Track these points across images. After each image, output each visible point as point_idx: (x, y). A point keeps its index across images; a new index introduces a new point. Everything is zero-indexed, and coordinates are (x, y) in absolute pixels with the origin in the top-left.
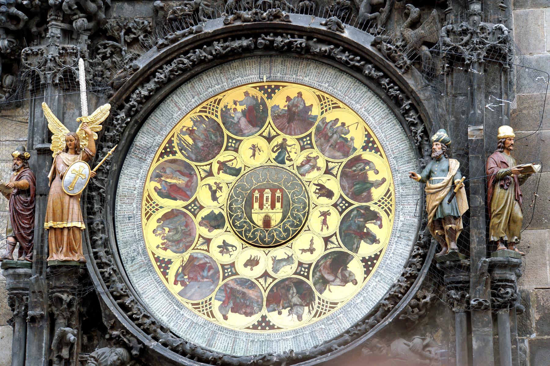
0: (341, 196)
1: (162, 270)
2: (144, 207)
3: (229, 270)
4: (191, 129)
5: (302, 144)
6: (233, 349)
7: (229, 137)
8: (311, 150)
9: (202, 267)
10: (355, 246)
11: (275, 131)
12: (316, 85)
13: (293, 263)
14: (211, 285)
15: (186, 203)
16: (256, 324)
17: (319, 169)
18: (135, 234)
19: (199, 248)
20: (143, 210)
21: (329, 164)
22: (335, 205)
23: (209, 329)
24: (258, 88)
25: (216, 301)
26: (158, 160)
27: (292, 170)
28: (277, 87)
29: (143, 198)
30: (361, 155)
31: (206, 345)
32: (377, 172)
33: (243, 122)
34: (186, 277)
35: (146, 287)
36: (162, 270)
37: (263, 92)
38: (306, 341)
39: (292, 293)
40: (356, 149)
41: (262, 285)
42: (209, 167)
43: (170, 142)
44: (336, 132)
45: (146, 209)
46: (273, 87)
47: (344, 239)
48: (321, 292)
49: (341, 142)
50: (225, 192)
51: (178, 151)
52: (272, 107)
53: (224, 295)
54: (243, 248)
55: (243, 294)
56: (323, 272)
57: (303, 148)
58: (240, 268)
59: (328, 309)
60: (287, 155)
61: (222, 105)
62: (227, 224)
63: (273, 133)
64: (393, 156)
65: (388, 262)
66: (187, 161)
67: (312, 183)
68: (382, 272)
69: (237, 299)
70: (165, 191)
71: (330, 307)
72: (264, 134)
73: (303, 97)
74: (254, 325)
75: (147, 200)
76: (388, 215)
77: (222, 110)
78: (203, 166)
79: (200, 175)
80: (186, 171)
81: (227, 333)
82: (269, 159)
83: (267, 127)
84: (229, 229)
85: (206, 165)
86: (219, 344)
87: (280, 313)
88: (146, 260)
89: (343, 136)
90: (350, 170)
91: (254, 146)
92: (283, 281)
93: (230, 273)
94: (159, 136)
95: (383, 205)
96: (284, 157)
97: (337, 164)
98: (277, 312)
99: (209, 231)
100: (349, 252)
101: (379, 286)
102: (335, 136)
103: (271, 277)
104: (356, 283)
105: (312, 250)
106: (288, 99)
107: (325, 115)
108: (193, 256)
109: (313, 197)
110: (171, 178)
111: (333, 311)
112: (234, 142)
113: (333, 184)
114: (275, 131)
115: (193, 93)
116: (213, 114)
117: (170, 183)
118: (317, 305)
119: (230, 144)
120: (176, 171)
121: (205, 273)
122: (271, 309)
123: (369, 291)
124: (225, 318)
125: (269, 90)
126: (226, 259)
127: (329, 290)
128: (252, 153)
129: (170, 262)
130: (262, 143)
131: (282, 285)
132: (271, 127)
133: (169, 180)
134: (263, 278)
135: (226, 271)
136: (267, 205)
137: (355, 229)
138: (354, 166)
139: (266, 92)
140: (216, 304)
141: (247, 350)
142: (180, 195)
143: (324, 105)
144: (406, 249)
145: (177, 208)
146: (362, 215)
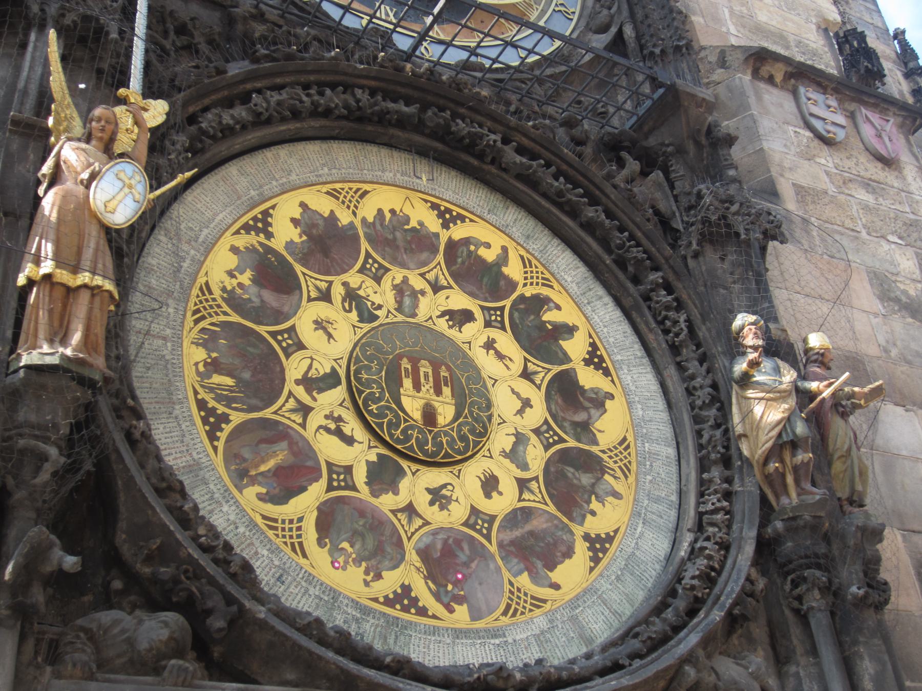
2: (279, 541)
3: (480, 522)
4: (209, 360)
6: (615, 613)
7: (273, 334)
10: (561, 355)
12: (314, 179)
14: (488, 565)
15: (323, 483)
17: (423, 293)
18: (317, 597)
19: (412, 530)
20: (283, 547)
21: (427, 276)
22: (488, 324)
23: (563, 622)
25: (519, 578)
26: (215, 449)
27: (395, 320)
28: (266, 213)
30: (450, 237)
31: (587, 646)
32: (488, 246)
33: (269, 297)
34: (450, 587)
39: (573, 475)
41: (534, 501)
42: (292, 400)
44: (395, 229)
45: (285, 543)
48: (595, 442)
51: (227, 411)
53: (515, 560)
55: (532, 535)
56: (568, 418)
57: (378, 280)
60: (369, 304)
61: (217, 293)
64: (486, 212)
67: (434, 318)
70: (277, 490)
72: (313, 294)
73: (310, 207)
74: (591, 559)
75: (271, 528)
78: (283, 405)
79: (294, 421)
82: (354, 326)
83: (306, 281)
84: (414, 467)
85: (286, 401)
86: (595, 626)
87: (593, 513)
88: (379, 619)
89: (406, 227)
91: (316, 322)
94: (177, 407)
95: (535, 280)
97: (435, 270)
98: (589, 516)
100: (564, 367)
102: (398, 235)
105: (527, 403)
106: (295, 222)
107: (360, 215)
109: (453, 333)
110: (263, 461)
113: (459, 300)
117: (269, 471)
118: (611, 461)
119: (284, 344)
120: (257, 445)
121: (463, 557)
122: (579, 519)
124: (556, 587)
125: (260, 225)
127: (600, 431)
128: (323, 334)
129: (406, 589)
130: (320, 310)
132: (311, 277)
133: (263, 468)
134: (525, 490)
138: (456, 257)
139: (258, 231)
140: (524, 580)
141: (627, 595)
145: (322, 500)
146: (527, 312)
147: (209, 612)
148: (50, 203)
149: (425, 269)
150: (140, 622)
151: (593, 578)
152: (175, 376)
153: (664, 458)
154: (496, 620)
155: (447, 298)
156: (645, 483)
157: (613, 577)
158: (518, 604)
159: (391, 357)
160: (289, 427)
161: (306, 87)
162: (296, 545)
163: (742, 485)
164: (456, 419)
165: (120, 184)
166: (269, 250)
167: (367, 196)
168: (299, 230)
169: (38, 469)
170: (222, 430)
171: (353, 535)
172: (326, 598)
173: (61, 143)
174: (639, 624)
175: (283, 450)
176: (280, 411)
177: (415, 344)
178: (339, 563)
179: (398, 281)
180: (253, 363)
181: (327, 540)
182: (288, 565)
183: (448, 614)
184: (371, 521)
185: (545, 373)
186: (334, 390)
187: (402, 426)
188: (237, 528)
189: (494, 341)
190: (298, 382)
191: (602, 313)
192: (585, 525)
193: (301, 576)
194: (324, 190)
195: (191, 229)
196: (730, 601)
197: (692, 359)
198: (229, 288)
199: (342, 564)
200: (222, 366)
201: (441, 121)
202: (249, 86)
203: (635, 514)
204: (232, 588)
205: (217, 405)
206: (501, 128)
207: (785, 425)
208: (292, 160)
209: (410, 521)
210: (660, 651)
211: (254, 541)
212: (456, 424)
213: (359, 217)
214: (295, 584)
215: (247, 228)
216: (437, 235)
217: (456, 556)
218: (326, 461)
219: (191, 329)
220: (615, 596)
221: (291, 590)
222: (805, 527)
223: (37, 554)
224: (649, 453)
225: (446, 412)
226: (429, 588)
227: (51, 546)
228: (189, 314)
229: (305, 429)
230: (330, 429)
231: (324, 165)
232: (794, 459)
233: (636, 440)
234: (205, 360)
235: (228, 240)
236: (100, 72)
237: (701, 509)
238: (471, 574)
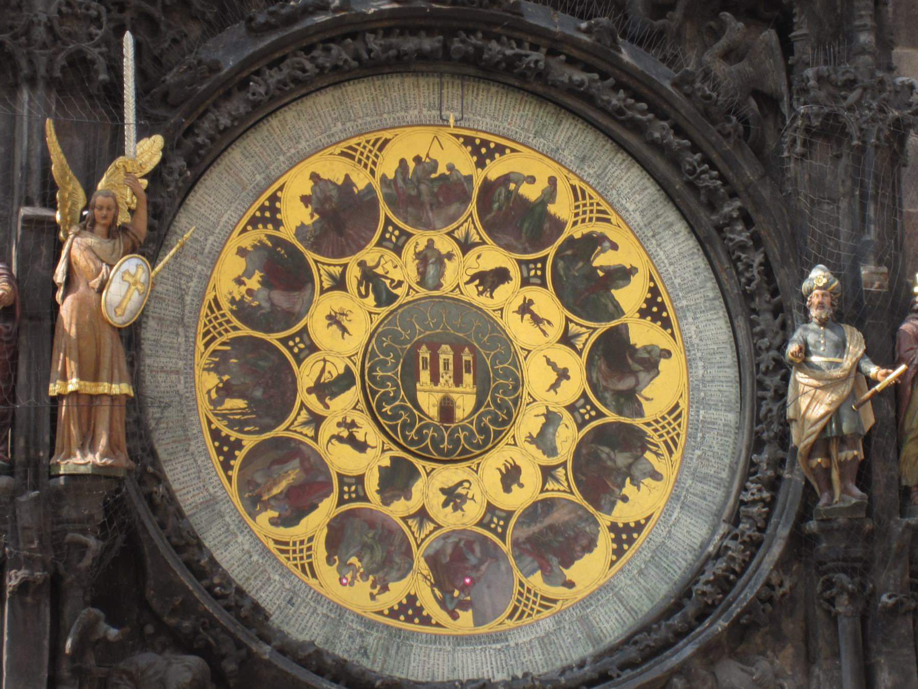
1: (417, 620)
2: (290, 565)
3: (495, 520)
4: (221, 385)
5: (391, 246)
6: (630, 610)
7: (284, 341)
8: (412, 241)
9: (459, 555)
10: (611, 308)
11: (335, 265)
13: (561, 418)
14: (498, 567)
15: (334, 497)
16: (615, 546)
17: (450, 256)
18: (324, 615)
19: (423, 536)
20: (293, 569)
22: (525, 282)
24: (249, 228)
25: (531, 578)
26: (229, 478)
27: (417, 296)
28: (274, 198)
29: (273, 555)
30: (486, 178)
31: (594, 647)
32: (532, 180)
33: (279, 297)
34: (456, 593)
35: (427, 666)
37: (260, 226)
39: (608, 456)
41: (559, 491)
42: (304, 412)
43: (215, 434)
44: (419, 181)
45: (296, 565)
46: (267, 204)
48: (640, 413)
49: (440, 188)
50: (365, 422)
51: (240, 436)
52: (297, 234)
53: (529, 559)
54: (477, 472)
56: (611, 387)
57: (398, 250)
59: (674, 425)
60: (388, 282)
61: (226, 306)
62: (419, 464)
63: (337, 271)
64: (532, 136)
65: (677, 281)
68: (684, 303)
69: (552, 542)
70: (289, 512)
71: (675, 419)
73: (322, 176)
74: (615, 552)
75: (283, 551)
76: (608, 221)
77: (232, 311)
78: (295, 419)
81: (598, 600)
82: (370, 313)
83: (319, 270)
84: (429, 465)
85: (299, 414)
86: (606, 625)
87: (625, 499)
89: (433, 176)
90: (493, 214)
91: (330, 317)
92: (577, 454)
95: (588, 215)
97: (466, 225)
98: (620, 503)
102: (424, 188)
105: (563, 375)
106: (305, 200)
110: (275, 484)
111: (683, 420)
115: (171, 329)
117: (281, 492)
118: (655, 435)
120: (269, 468)
121: (473, 560)
122: (607, 507)
123: (698, 345)
124: (570, 585)
125: (267, 214)
126: (473, 511)
127: (647, 399)
128: (339, 329)
129: (412, 599)
132: (324, 264)
133: (276, 491)
134: (549, 479)
136: (446, 378)
137: (586, 287)
138: (492, 202)
139: (264, 221)
140: (536, 581)
141: (648, 590)
143: (364, 160)
144: (680, 241)
145: (332, 516)
146: (574, 258)
147: (223, 657)
148: (67, 309)
149: (455, 225)
150: (169, 664)
151: (613, 572)
152: (190, 410)
153: (721, 427)
154: (501, 624)
155: (479, 257)
156: (691, 459)
157: (635, 572)
158: (526, 605)
159: (409, 346)
161: (308, 49)
162: (306, 566)
163: (791, 472)
164: (476, 409)
165: (126, 284)
166: (278, 242)
167: (388, 146)
168: (310, 209)
169: (82, 555)
170: (235, 458)
171: (361, 549)
172: (333, 616)
173: (69, 241)
174: (636, 633)
175: (294, 469)
176: (293, 428)
177: (436, 325)
178: (347, 579)
179: (421, 248)
180: (264, 377)
181: (336, 557)
182: (298, 588)
184: (380, 532)
185: (589, 333)
186: (348, 392)
187: (417, 426)
188: (251, 557)
189: (531, 302)
190: (310, 391)
191: (671, 246)
193: (310, 596)
194: (338, 151)
195: (197, 240)
196: (739, 610)
197: (765, 311)
198: (238, 298)
199: (350, 580)
200: (234, 388)
201: (471, 49)
202: (245, 74)
203: (674, 497)
204: (241, 633)
206: (543, 42)
207: (831, 419)
208: (300, 122)
209: (421, 527)
210: (652, 662)
211: (267, 567)
212: (476, 415)
213: (378, 175)
214: (304, 604)
215: (254, 222)
216: (469, 179)
218: (338, 473)
219: (202, 354)
220: (634, 592)
221: (301, 610)
222: (838, 530)
223: (89, 627)
224: (704, 422)
225: (465, 402)
227: (97, 620)
228: (200, 337)
229: (317, 442)
232: (840, 455)
233: (689, 406)
234: (217, 386)
236: (90, 97)
237: (741, 497)
238: (479, 578)
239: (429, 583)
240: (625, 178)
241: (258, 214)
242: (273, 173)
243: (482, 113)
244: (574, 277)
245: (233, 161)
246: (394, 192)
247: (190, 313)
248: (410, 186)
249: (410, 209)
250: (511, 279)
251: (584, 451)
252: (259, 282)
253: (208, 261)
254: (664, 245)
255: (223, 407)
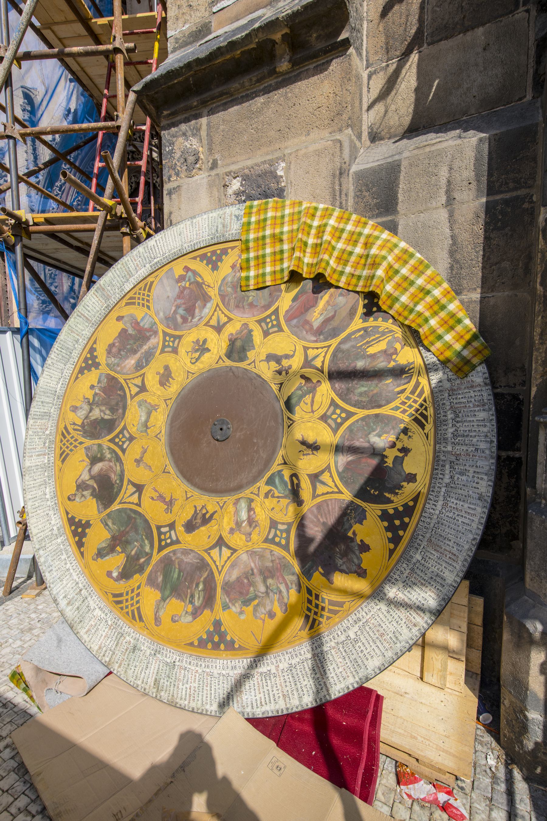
0: (178, 542)
3: (171, 344)
4: (394, 357)
5: (280, 527)
7: (350, 415)
9: (190, 311)
10: (110, 523)
11: (323, 494)
16: (95, 354)
24: (411, 504)
28: (396, 540)
34: (187, 285)
35: (197, 229)
36: (209, 254)
37: (401, 509)
38: (44, 404)
40: (224, 610)
44: (267, 593)
46: (401, 533)
47: (126, 513)
48: (87, 449)
49: (248, 593)
51: (366, 325)
52: (364, 511)
53: (146, 327)
54: (188, 372)
55: (135, 351)
56: (106, 463)
58: (170, 359)
64: (177, 663)
65: (63, 557)
66: (343, 335)
68: (59, 540)
71: (64, 451)
78: (324, 357)
79: (313, 348)
80: (329, 327)
83: (336, 486)
89: (256, 602)
90: (202, 579)
92: (125, 408)
93: (167, 344)
96: (276, 487)
99: (232, 334)
100: (108, 511)
101: (48, 526)
102: (262, 589)
103: (137, 394)
104: (69, 499)
106: (365, 548)
108: (209, 301)
110: (328, 302)
112: (339, 420)
114: (323, 494)
116: (404, 403)
118: (76, 437)
119: (338, 411)
120: (335, 312)
121: (181, 311)
123: (49, 510)
125: (397, 522)
127: (83, 461)
129: (215, 268)
131: (121, 404)
134: (140, 384)
135: (172, 339)
138: (203, 590)
139: (398, 514)
141: (72, 332)
142: (297, 309)
146: (137, 557)
156: (52, 426)
160: (316, 341)
183: (187, 265)
192: (99, 375)
195: (462, 474)
205: (375, 324)
208: (392, 629)
215: (408, 510)
217: (185, 310)
226: (200, 276)
230: (286, 358)
231: (356, 641)
234: (397, 355)
235: (421, 484)
239: (206, 283)
240: (102, 638)
241: (406, 520)
242: (405, 565)
243: (221, 677)
244: (137, 541)
245: (450, 568)
246: (286, 577)
247: (443, 404)
248: (274, 587)
249: (269, 564)
250: (183, 525)
251: (120, 411)
252: (386, 457)
253: (444, 458)
254: (74, 584)
255: (387, 340)
